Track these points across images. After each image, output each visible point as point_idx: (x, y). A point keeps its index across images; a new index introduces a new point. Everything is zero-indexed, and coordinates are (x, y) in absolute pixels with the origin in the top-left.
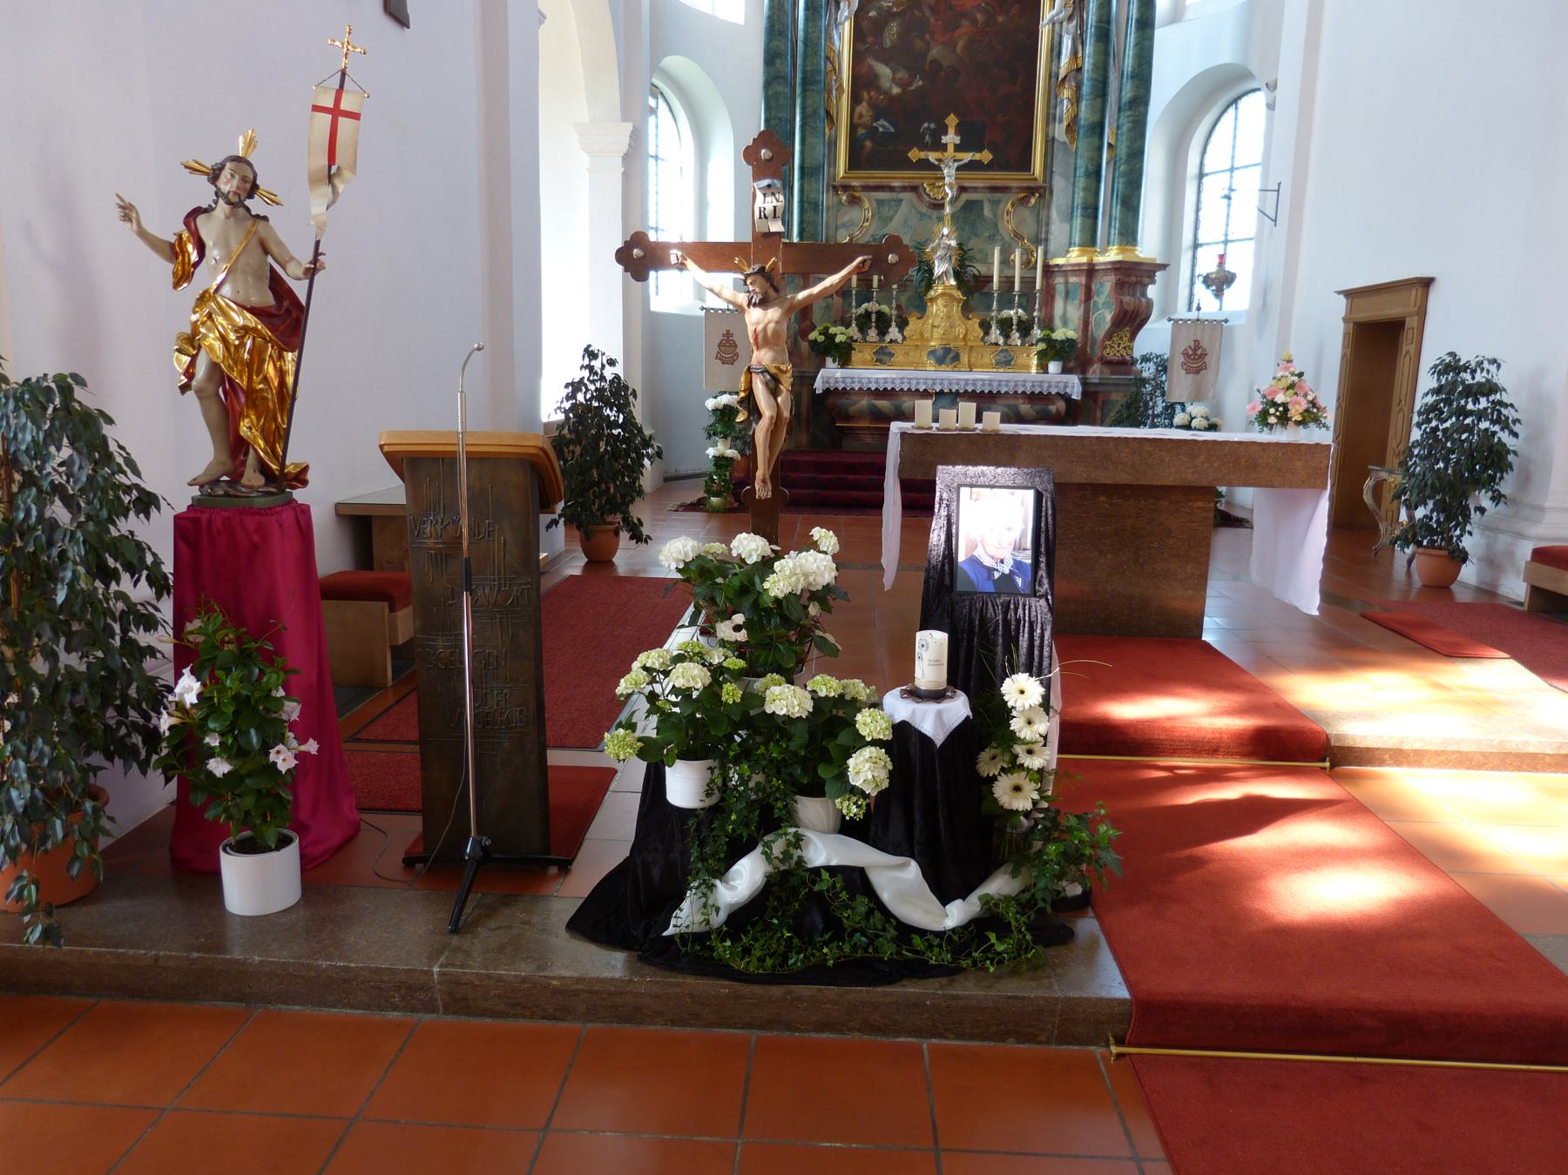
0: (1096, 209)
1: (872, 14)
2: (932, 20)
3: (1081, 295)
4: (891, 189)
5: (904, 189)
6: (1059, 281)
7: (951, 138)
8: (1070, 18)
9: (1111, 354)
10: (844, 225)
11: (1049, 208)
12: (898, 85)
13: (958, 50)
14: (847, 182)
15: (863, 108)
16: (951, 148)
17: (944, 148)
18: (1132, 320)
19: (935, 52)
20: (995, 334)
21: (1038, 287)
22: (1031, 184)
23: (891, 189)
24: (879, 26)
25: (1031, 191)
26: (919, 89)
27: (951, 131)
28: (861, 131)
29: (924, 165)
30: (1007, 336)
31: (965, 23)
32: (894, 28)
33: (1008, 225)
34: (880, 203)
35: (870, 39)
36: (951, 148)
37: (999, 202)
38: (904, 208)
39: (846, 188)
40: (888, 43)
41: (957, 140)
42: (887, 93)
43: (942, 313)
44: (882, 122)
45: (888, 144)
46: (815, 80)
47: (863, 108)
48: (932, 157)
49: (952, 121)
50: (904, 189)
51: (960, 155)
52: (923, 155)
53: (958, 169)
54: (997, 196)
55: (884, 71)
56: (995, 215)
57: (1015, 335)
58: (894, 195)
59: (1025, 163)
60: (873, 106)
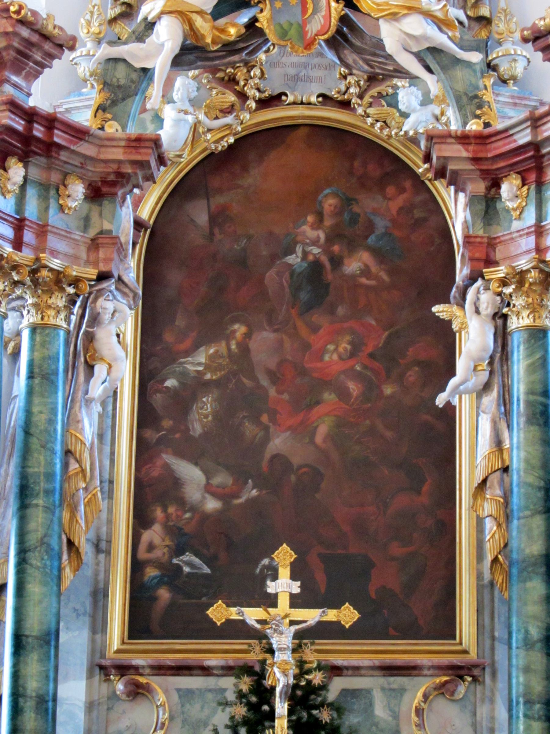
1: (171, 383)
2: (272, 392)
4: (206, 671)
7: (284, 586)
8: (487, 387)
11: (492, 701)
12: (216, 495)
13: (319, 439)
14: (125, 658)
15: (154, 534)
16: (284, 602)
17: (271, 601)
19: (279, 443)
22: (456, 659)
23: (206, 671)
24: (183, 401)
25: (459, 672)
26: (252, 502)
27: (284, 573)
28: (151, 573)
29: (237, 630)
31: (329, 397)
32: (206, 407)
34: (187, 695)
35: (167, 423)
36: (284, 602)
37: (402, 691)
39: (123, 669)
40: (197, 429)
41: (296, 588)
44: (188, 557)
48: (252, 615)
49: (284, 556)
51: (300, 614)
52: (233, 613)
53: (298, 635)
54: (397, 681)
55: (191, 474)
56: (396, 716)
58: (210, 682)
59: (447, 628)
60: (172, 530)
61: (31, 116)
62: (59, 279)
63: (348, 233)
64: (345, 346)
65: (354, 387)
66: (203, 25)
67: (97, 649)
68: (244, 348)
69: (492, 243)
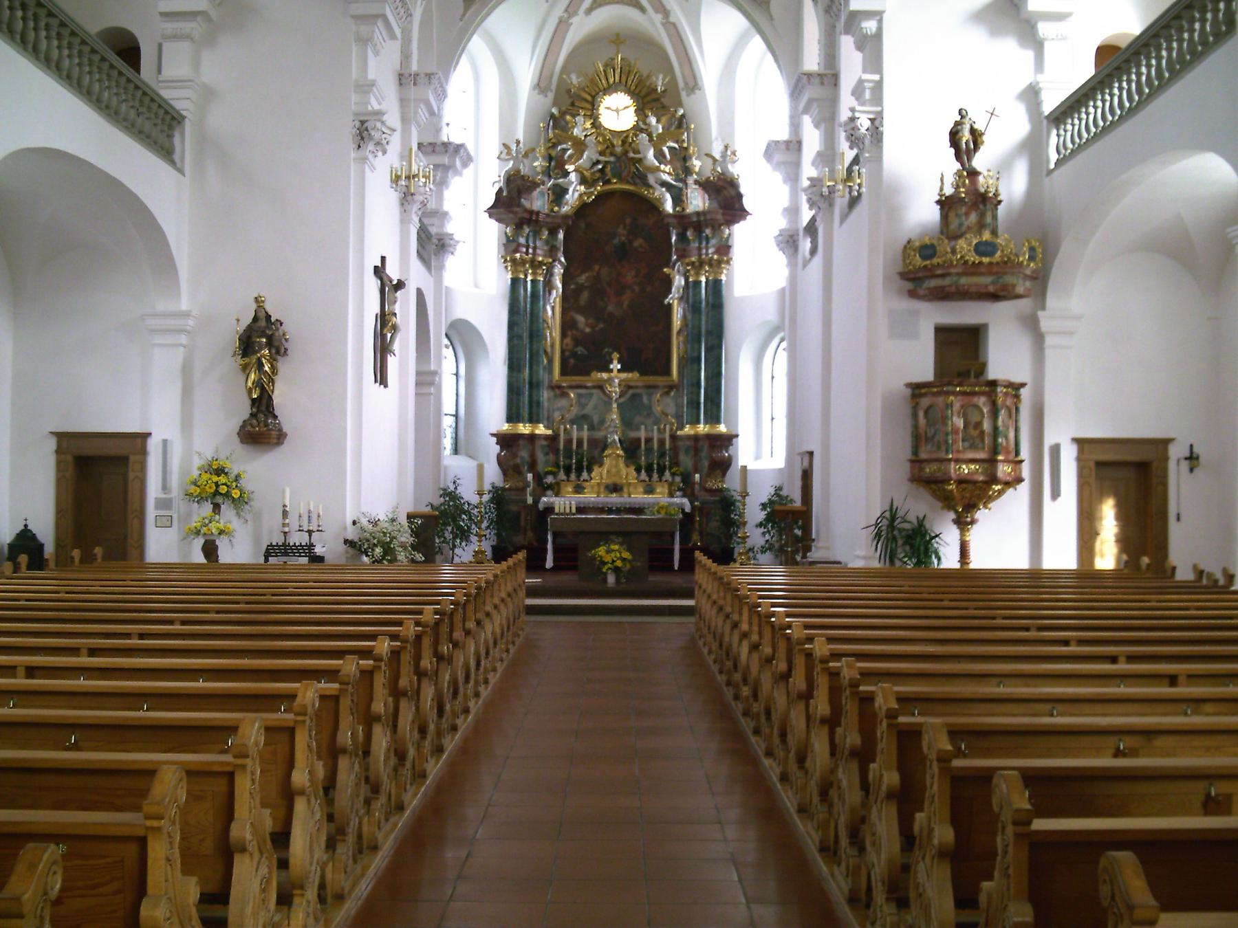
0: (699, 404)
3: (692, 453)
4: (586, 387)
5: (594, 387)
6: (680, 444)
9: (710, 484)
10: (558, 409)
15: (568, 340)
16: (615, 371)
17: (611, 371)
18: (723, 466)
19: (611, 308)
20: (643, 475)
21: (667, 446)
23: (586, 387)
25: (671, 387)
27: (615, 362)
28: (567, 354)
30: (650, 476)
31: (628, 292)
32: (585, 296)
33: (657, 409)
36: (615, 371)
38: (595, 399)
39: (559, 387)
42: (582, 331)
43: (613, 466)
45: (583, 359)
46: (535, 334)
47: (568, 340)
48: (605, 375)
49: (616, 355)
50: (594, 387)
54: (651, 391)
55: (581, 319)
57: (655, 476)
59: (667, 371)
61: (531, 212)
62: (541, 263)
63: (634, 231)
64: (633, 273)
65: (637, 289)
66: (587, 174)
67: (551, 381)
68: (598, 273)
69: (684, 250)
